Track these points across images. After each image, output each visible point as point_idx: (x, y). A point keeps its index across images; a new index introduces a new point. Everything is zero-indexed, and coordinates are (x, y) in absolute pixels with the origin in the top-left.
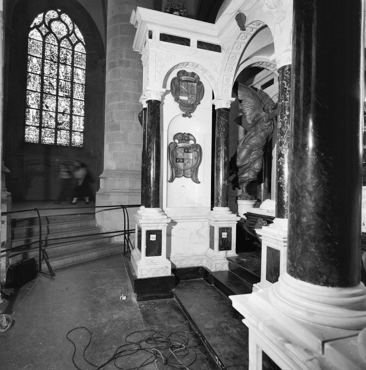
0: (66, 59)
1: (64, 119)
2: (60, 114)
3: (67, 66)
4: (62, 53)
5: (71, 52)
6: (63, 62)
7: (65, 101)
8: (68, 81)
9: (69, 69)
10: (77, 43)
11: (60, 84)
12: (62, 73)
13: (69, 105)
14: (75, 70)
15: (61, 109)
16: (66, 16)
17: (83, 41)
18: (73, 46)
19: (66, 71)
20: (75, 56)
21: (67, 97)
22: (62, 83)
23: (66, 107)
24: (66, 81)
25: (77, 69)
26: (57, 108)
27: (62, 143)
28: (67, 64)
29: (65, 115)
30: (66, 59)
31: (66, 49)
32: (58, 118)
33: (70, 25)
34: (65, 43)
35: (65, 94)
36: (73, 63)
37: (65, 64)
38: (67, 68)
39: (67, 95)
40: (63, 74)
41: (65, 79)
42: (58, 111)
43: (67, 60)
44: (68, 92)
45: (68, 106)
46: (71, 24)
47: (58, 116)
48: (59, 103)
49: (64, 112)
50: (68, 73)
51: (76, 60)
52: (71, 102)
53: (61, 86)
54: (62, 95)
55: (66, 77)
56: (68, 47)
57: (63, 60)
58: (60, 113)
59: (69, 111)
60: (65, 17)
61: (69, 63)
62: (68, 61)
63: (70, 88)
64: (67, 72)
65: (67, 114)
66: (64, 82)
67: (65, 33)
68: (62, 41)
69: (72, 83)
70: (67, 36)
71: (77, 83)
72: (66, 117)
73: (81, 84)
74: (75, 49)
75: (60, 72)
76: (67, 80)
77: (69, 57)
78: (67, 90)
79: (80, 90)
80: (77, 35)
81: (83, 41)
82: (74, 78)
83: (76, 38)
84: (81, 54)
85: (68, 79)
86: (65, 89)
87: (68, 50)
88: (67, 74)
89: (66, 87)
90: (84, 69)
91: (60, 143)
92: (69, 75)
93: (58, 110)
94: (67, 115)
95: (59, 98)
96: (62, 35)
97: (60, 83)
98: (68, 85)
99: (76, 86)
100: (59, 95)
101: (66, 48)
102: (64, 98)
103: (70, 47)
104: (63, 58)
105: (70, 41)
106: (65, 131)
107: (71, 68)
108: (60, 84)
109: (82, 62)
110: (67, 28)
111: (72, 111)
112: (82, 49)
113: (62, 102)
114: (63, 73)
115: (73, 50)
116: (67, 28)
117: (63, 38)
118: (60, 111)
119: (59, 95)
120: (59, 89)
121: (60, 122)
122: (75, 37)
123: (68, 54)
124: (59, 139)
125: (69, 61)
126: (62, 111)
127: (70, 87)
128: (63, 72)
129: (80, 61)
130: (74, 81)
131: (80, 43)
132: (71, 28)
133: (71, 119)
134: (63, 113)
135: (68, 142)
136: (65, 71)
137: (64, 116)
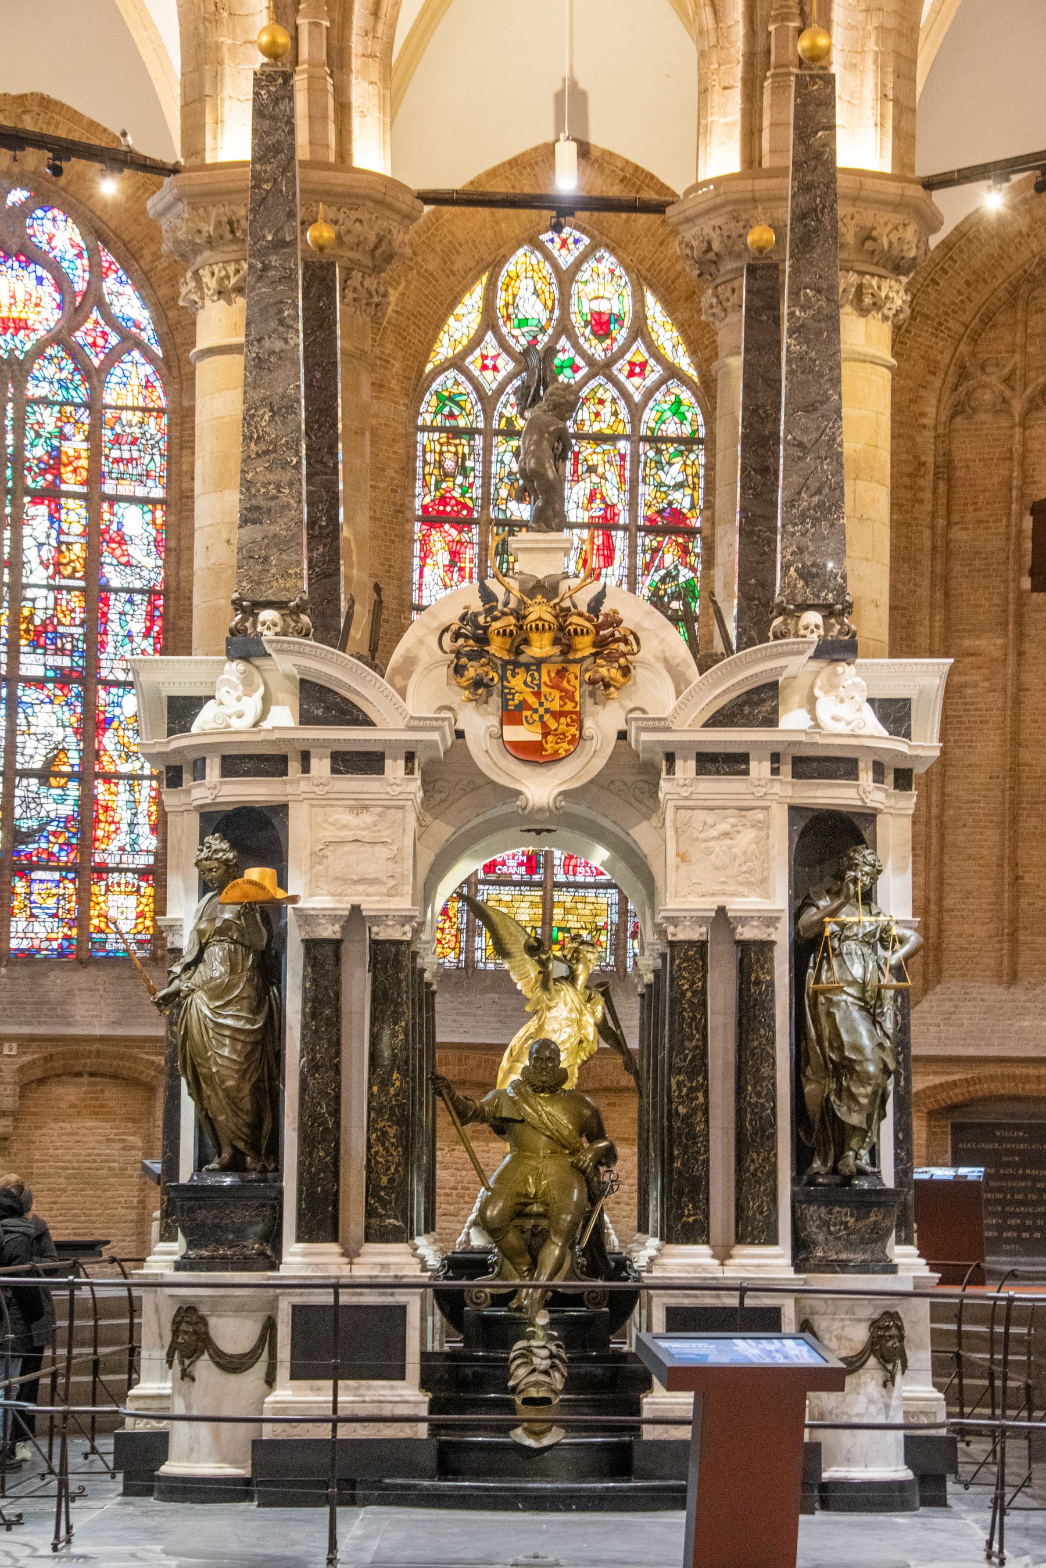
0: (58, 458)
1: (49, 807)
2: (25, 782)
3: (63, 501)
4: (38, 435)
5: (84, 415)
6: (41, 483)
7: (52, 702)
8: (69, 589)
9: (74, 514)
10: (113, 357)
11: (26, 612)
12: (40, 545)
13: (73, 719)
14: (106, 516)
15: (33, 754)
16: (54, 220)
17: (147, 335)
18: (94, 377)
19: (60, 532)
20: (107, 434)
21: (63, 679)
22: (40, 602)
23: (59, 734)
24: (59, 589)
25: (120, 508)
26: (11, 749)
27: (36, 943)
28: (63, 487)
29: (52, 780)
30: (55, 463)
31: (57, 408)
32: (17, 801)
33: (78, 262)
34: (50, 370)
35: (51, 661)
36: (95, 477)
37: (51, 496)
38: (63, 511)
39: (61, 668)
40: (45, 553)
41: (53, 577)
42: (19, 766)
43: (63, 470)
44: (68, 646)
45: (69, 730)
46: (79, 256)
47: (18, 792)
48: (21, 719)
49: (50, 762)
50: (69, 544)
51: (115, 454)
52: (84, 705)
53: (30, 619)
54: (39, 672)
55: (57, 564)
56: (67, 389)
57: (43, 472)
58: (26, 774)
59: (74, 757)
60: (48, 225)
61: (71, 483)
62: (67, 473)
63: (81, 625)
64: (63, 538)
65: (61, 775)
66: (51, 596)
67: (46, 316)
68: (36, 366)
69: (96, 595)
70: (60, 338)
71: (117, 591)
72: (60, 792)
73: (141, 591)
74: (109, 398)
75: (28, 543)
76: (65, 582)
77: (76, 445)
78: (62, 636)
79: (137, 626)
80: (116, 310)
81: (147, 335)
82: (102, 564)
83: (107, 329)
84: (139, 414)
85: (71, 577)
86: (55, 631)
87: (69, 409)
88: (64, 548)
89: (60, 623)
90: (154, 502)
91: (25, 944)
92: (77, 549)
93: (19, 758)
94: (63, 781)
95: (20, 693)
96: (34, 330)
97: (29, 604)
98: (73, 611)
99: (117, 604)
100: (24, 671)
101: (55, 403)
102: (50, 686)
103: (76, 389)
104: (40, 460)
105: (74, 353)
106: (56, 875)
107: (83, 513)
108: (26, 612)
109: (148, 458)
110: (62, 283)
111: (92, 754)
112: (148, 385)
113: (37, 708)
114: (46, 547)
115: (94, 405)
116: (62, 283)
117: (38, 352)
118: (26, 766)
119: (24, 671)
120: (23, 642)
121: (25, 825)
122: (102, 322)
123: (68, 429)
124: (22, 925)
125: (75, 471)
126: (38, 764)
127: (79, 616)
128: (42, 539)
129: (136, 455)
130: (103, 581)
131: (136, 354)
132: (80, 286)
133: (87, 801)
134: (45, 775)
135: (66, 937)
136: (54, 534)
137: (50, 787)
